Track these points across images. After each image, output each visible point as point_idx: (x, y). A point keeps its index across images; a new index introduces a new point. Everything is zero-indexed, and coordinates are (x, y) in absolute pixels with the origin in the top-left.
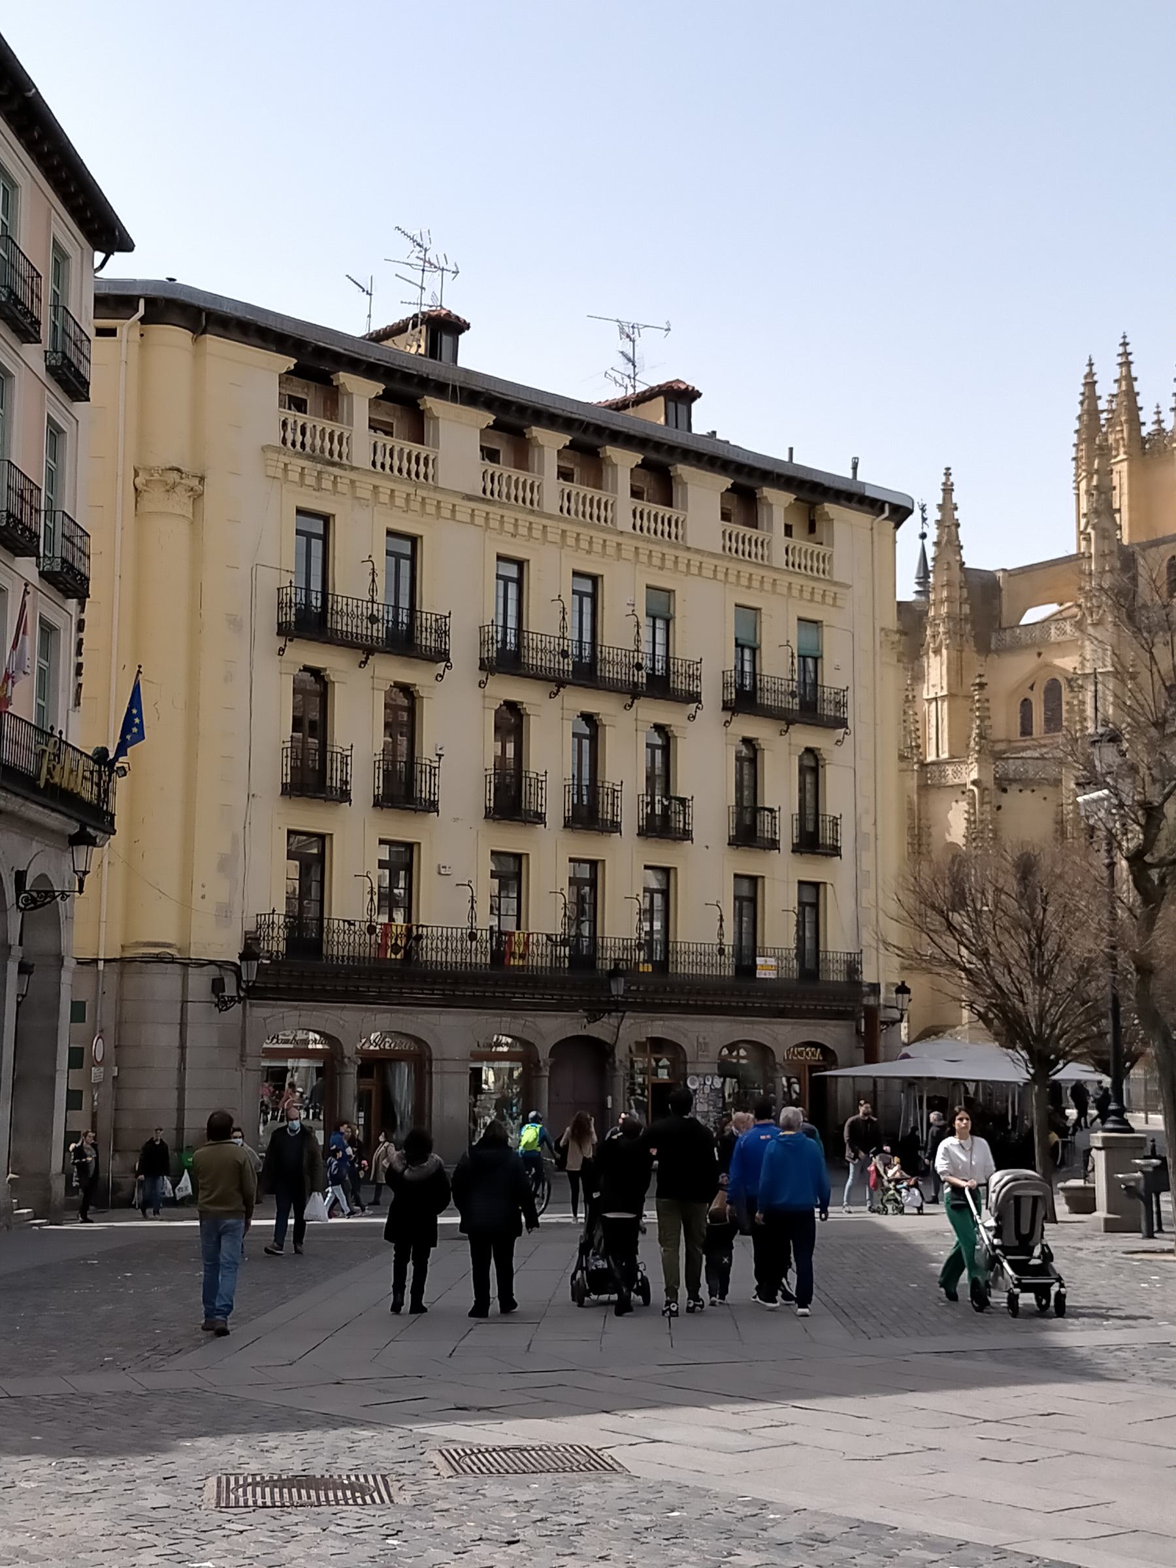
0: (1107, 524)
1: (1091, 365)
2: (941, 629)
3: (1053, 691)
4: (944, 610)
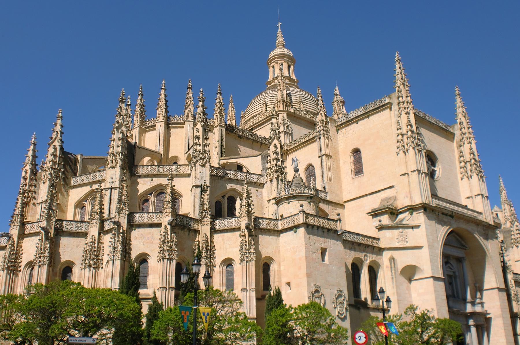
2: (48, 173)
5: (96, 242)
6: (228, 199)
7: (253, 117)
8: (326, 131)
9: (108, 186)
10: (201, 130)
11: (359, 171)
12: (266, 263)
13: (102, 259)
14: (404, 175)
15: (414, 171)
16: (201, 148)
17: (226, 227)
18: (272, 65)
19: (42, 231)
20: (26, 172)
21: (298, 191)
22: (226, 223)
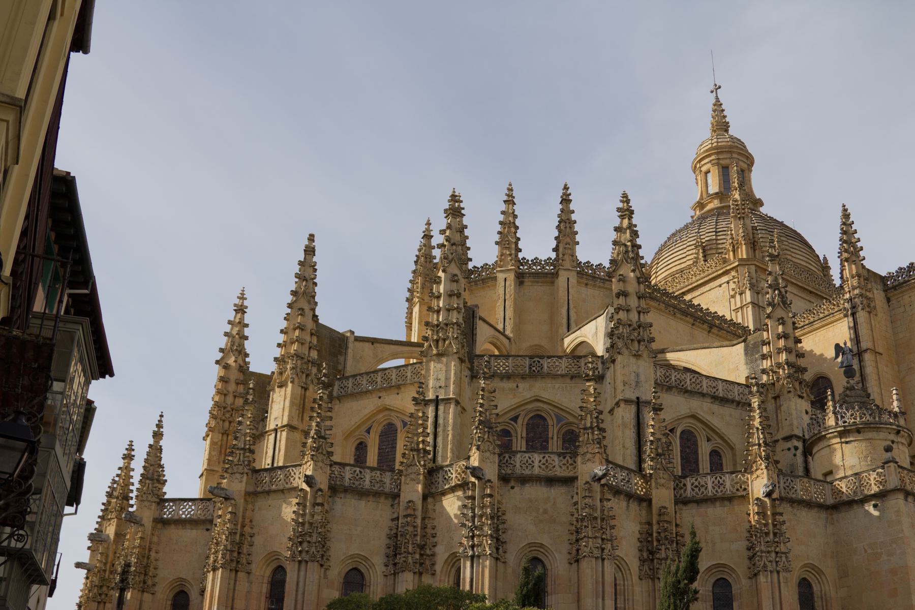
3: (389, 434)
5: (419, 513)
6: (681, 437)
7: (672, 275)
8: (868, 298)
9: (431, 396)
12: (804, 579)
13: (433, 555)
16: (634, 316)
17: (710, 494)
18: (704, 169)
19: (305, 486)
20: (226, 367)
21: (867, 418)
22: (710, 485)
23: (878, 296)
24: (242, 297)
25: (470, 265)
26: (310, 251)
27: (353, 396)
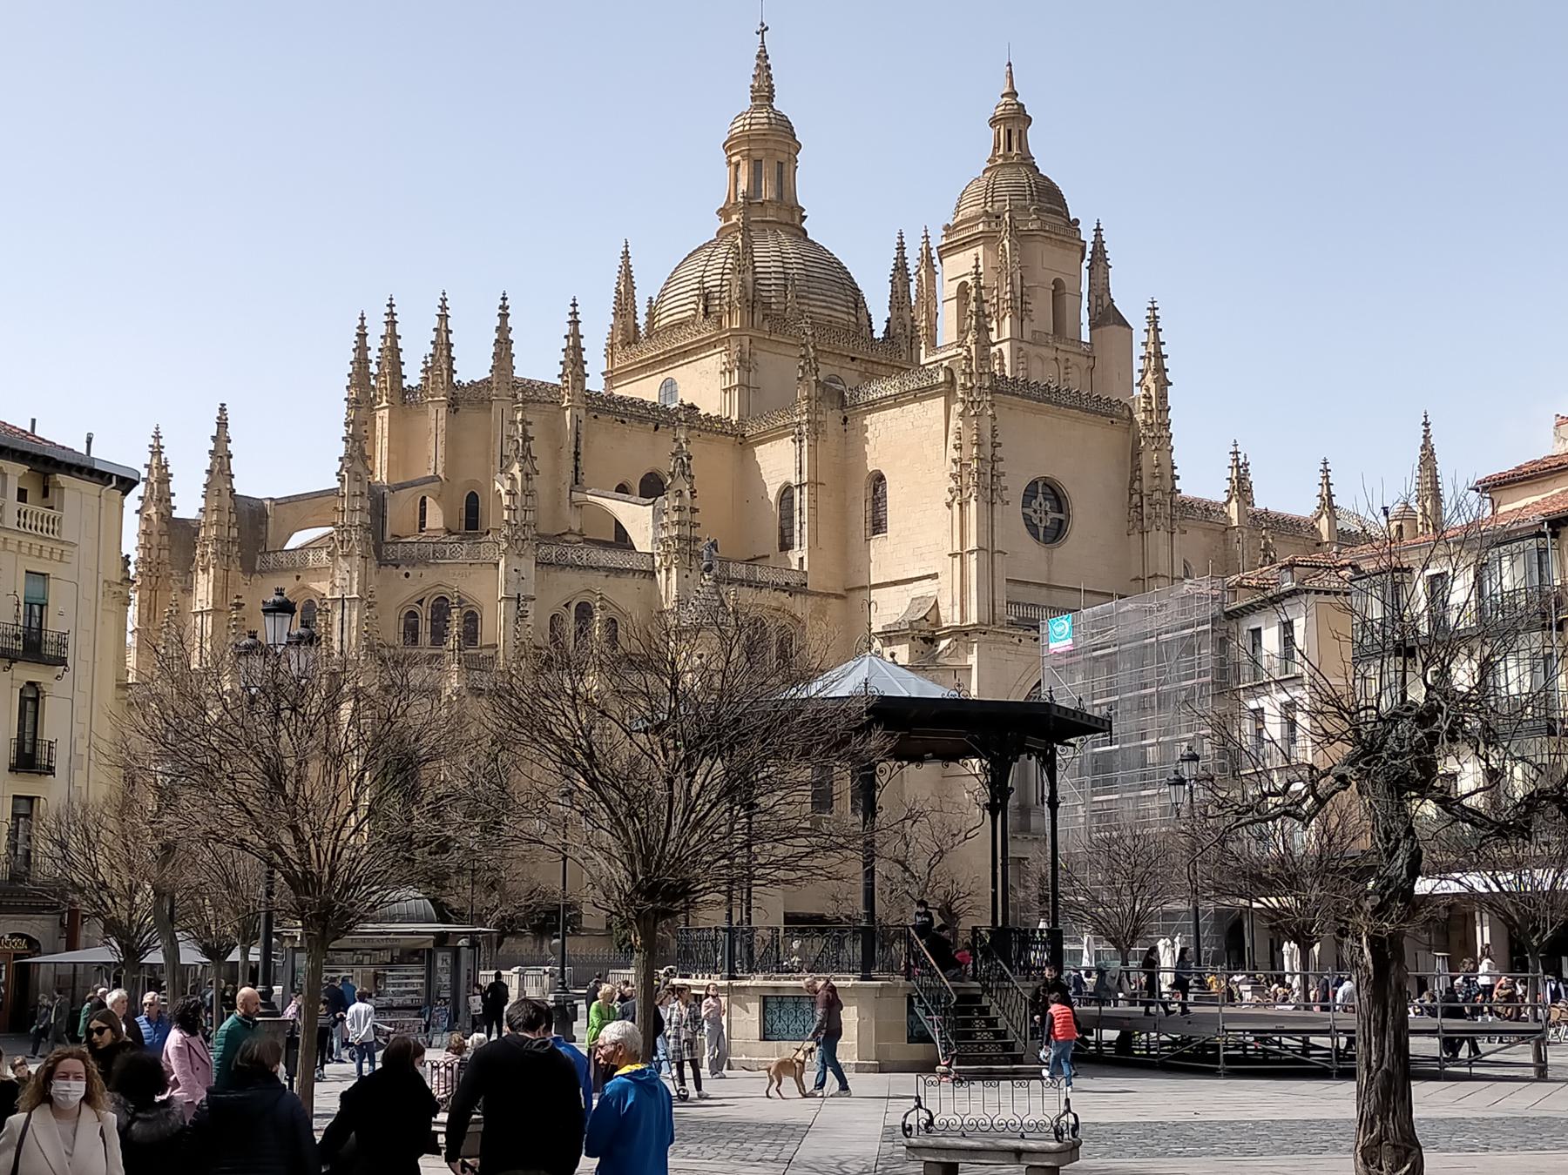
0: (361, 469)
1: (362, 319)
4: (213, 532)
10: (519, 476)
11: (878, 526)
14: (953, 555)
15: (971, 552)
20: (148, 519)
23: (832, 417)
24: (157, 437)
25: (405, 383)
26: (222, 424)
27: (273, 571)
